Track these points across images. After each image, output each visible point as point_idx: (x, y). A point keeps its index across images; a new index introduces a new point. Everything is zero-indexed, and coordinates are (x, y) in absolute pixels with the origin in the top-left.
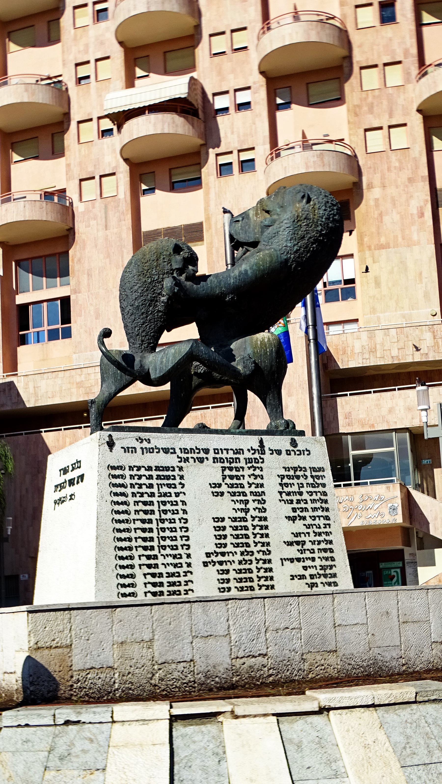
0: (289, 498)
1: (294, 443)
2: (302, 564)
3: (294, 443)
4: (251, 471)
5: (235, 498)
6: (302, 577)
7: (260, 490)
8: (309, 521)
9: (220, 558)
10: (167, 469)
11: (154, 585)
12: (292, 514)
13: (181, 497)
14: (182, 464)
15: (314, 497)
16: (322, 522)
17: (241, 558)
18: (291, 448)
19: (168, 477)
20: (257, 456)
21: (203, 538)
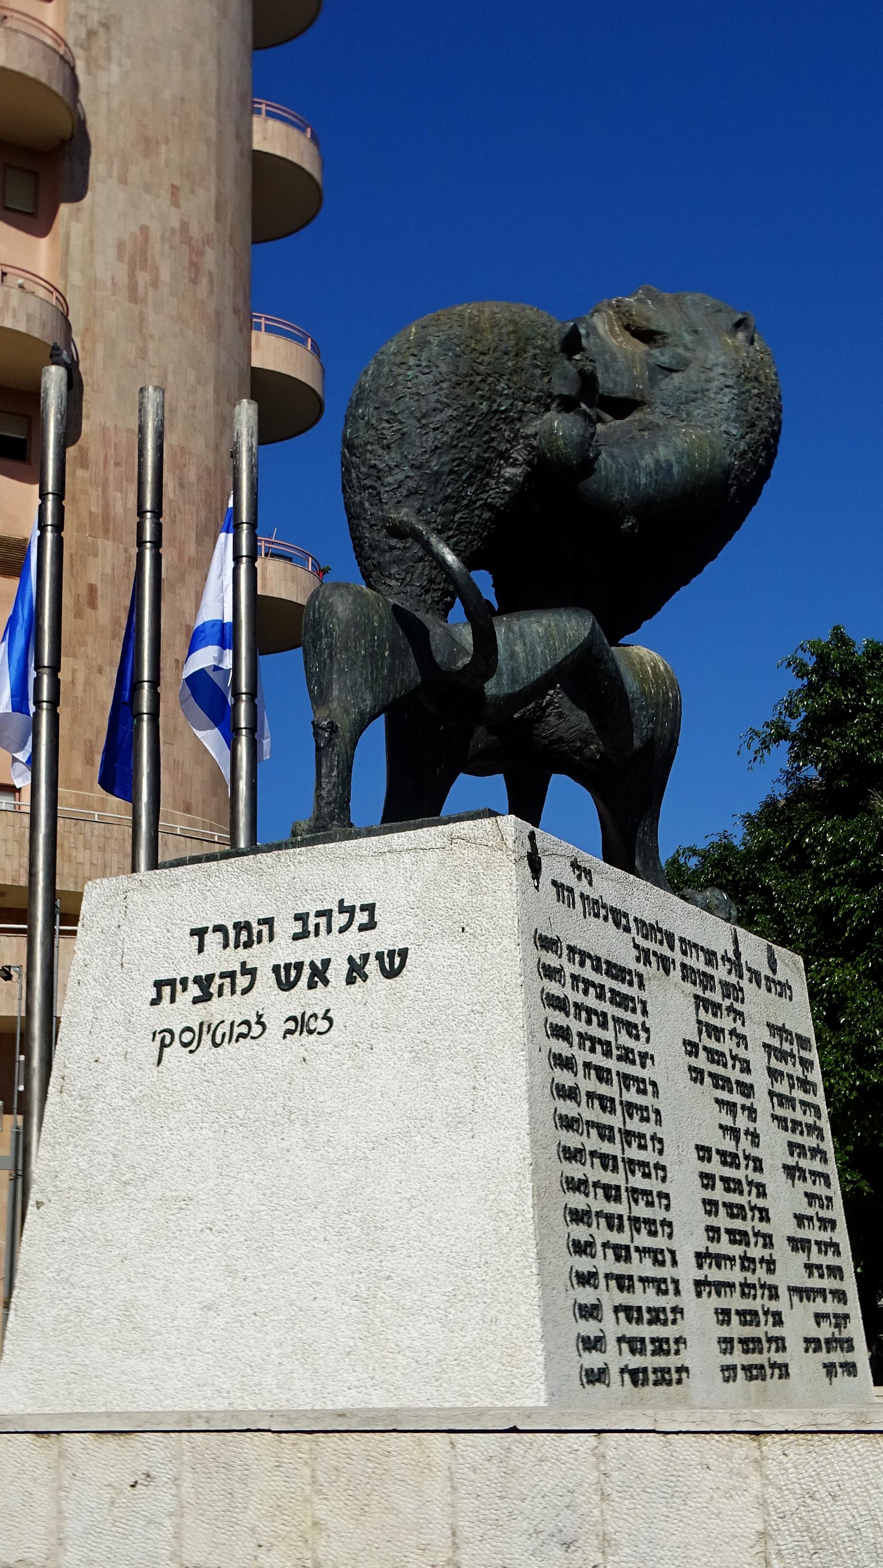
18: (770, 975)
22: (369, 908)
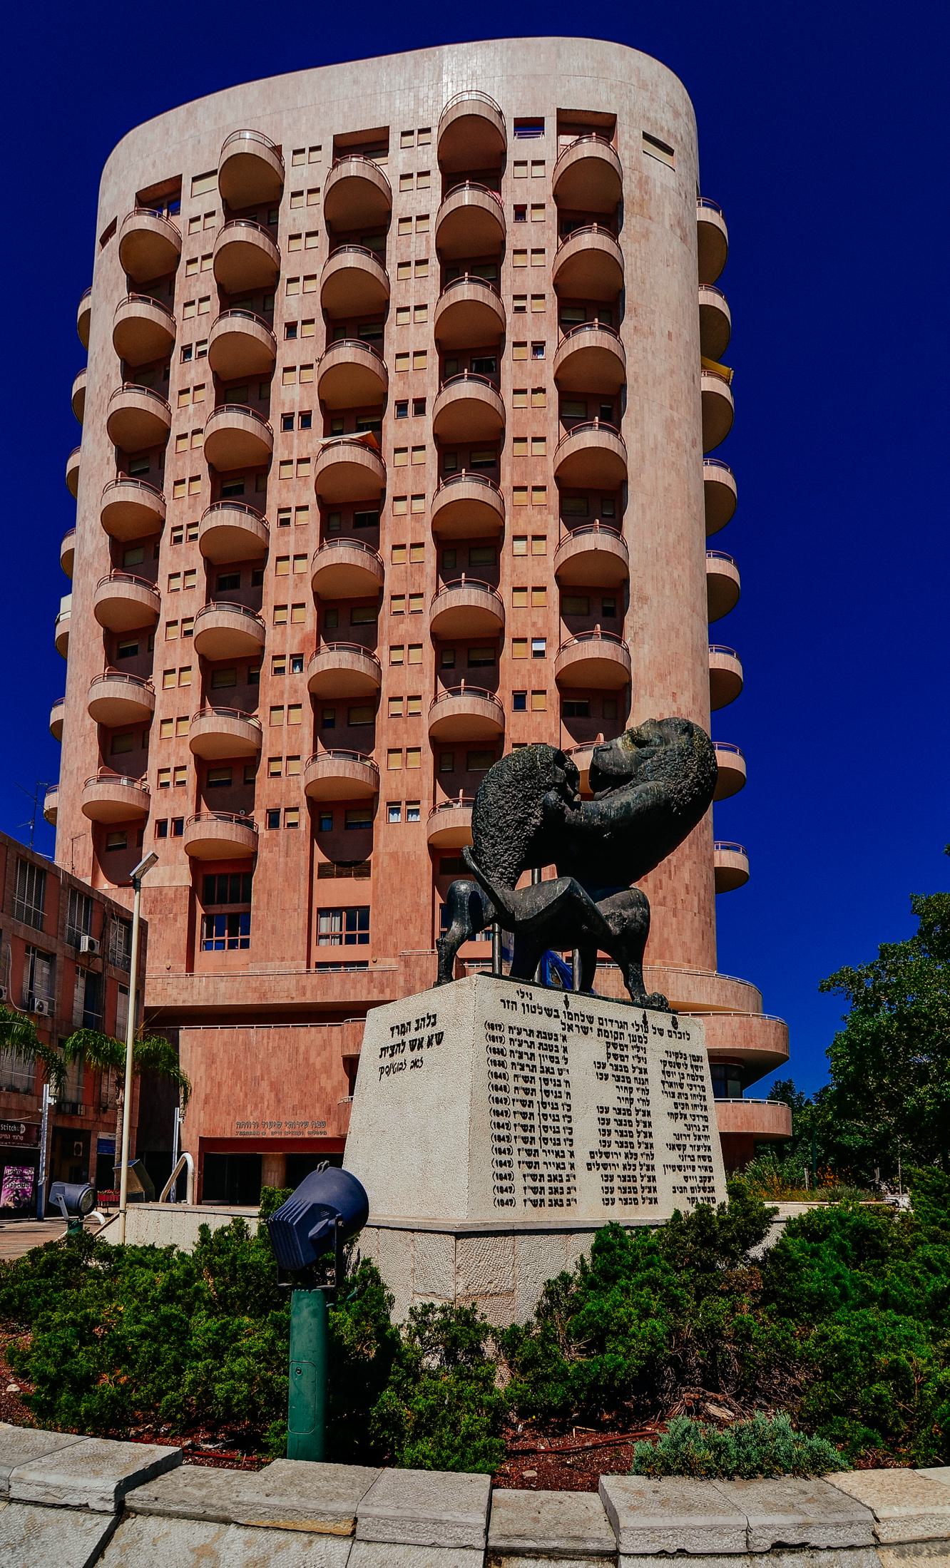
0: (671, 1090)
1: (675, 1024)
2: (683, 1173)
3: (675, 1024)
4: (635, 1052)
5: (620, 1084)
6: (683, 1189)
7: (644, 1076)
8: (689, 1121)
9: (604, 1160)
10: (549, 1036)
11: (534, 1190)
12: (675, 1111)
13: (565, 1076)
14: (566, 1032)
15: (694, 1092)
16: (700, 1122)
17: (625, 1162)
19: (550, 1048)
20: (641, 1033)
21: (586, 1135)
22: (435, 1016)
